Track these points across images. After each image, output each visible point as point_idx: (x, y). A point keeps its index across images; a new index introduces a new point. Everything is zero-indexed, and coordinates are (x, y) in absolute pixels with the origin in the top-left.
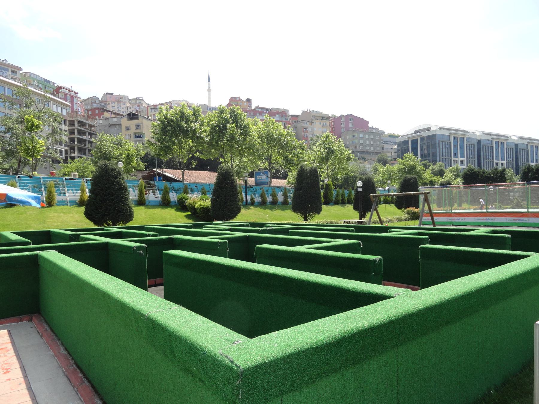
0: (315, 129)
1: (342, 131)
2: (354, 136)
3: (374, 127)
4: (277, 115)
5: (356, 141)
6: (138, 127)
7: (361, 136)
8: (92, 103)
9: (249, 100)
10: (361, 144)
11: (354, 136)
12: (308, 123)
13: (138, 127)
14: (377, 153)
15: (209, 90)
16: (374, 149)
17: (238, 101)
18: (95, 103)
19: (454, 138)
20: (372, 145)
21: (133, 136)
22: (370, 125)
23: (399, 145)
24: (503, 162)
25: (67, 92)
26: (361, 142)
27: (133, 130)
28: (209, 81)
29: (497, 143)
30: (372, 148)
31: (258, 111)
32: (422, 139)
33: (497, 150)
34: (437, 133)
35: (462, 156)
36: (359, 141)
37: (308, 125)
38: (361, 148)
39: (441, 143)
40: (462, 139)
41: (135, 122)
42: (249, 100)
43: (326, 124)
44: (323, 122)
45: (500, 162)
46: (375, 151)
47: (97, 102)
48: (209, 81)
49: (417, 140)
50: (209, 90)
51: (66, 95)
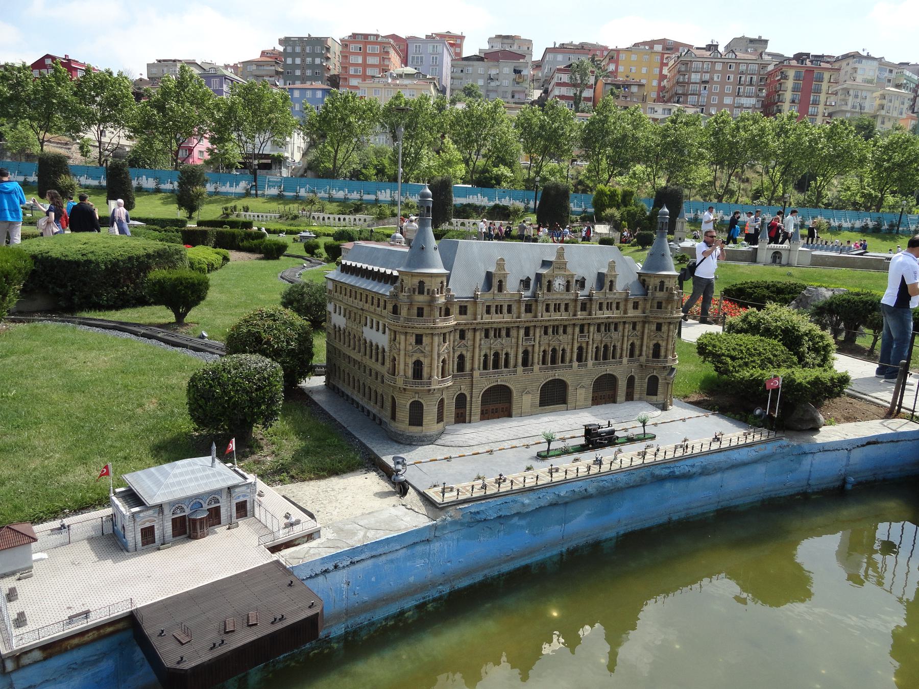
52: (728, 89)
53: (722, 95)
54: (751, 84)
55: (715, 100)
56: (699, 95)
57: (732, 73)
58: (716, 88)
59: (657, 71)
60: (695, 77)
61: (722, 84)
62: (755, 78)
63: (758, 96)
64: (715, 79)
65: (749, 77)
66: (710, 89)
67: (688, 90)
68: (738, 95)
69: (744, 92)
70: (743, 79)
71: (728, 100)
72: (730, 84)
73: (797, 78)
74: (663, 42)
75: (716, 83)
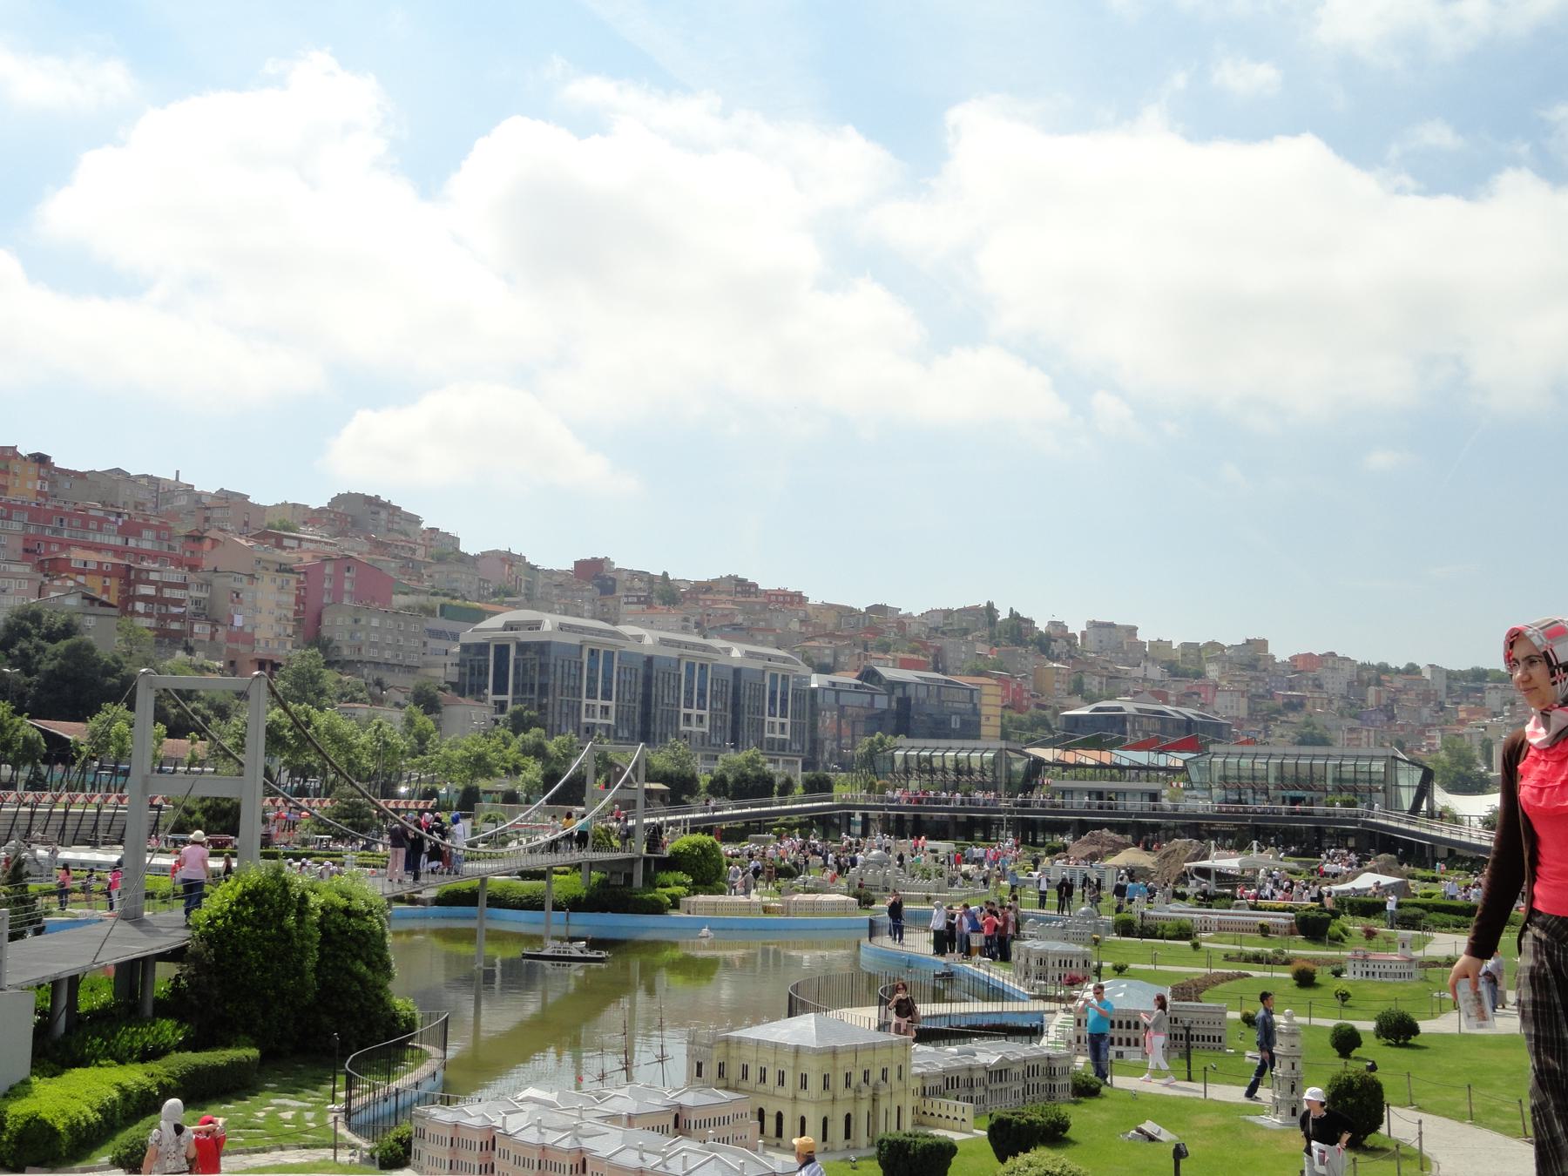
1: (326, 600)
3: (384, 499)
5: (361, 635)
7: (375, 622)
10: (374, 645)
12: (245, 579)
14: (411, 669)
17: (9, 459)
19: (592, 652)
23: (466, 648)
24: (701, 712)
26: (374, 637)
29: (690, 667)
32: (523, 647)
33: (689, 681)
34: (555, 639)
35: (607, 695)
37: (244, 584)
39: (560, 663)
40: (609, 656)
44: (280, 578)
45: (695, 712)
46: (407, 662)
49: (507, 647)
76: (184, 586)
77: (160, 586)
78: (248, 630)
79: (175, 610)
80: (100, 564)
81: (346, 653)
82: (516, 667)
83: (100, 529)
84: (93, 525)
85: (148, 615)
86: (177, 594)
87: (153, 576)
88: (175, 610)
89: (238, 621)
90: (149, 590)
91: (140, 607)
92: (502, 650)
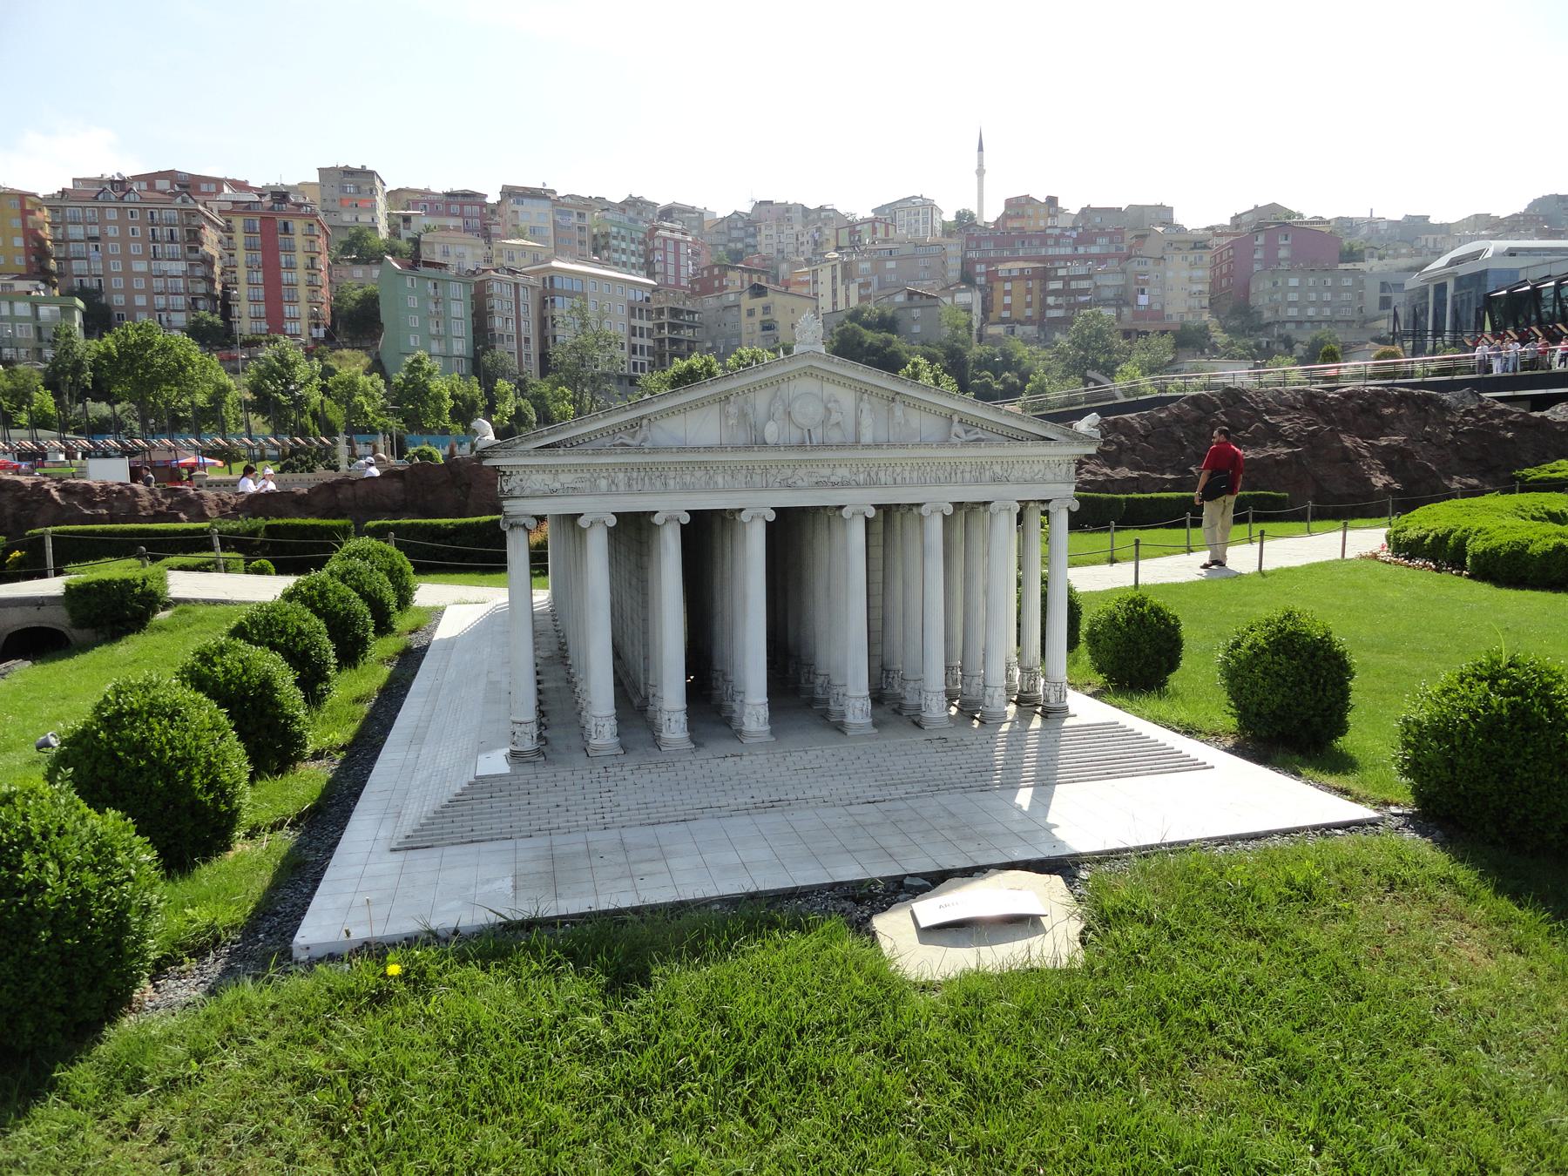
0: (1170, 274)
1: (1257, 267)
2: (1275, 284)
4: (1100, 241)
5: (1278, 297)
6: (766, 309)
7: (1294, 282)
8: (730, 228)
9: (1052, 201)
10: (1292, 304)
11: (1275, 284)
12: (1150, 262)
13: (766, 309)
15: (980, 172)
16: (1333, 313)
18: (736, 228)
20: (1327, 303)
21: (758, 327)
22: (1431, 220)
25: (667, 234)
26: (1293, 297)
27: (759, 316)
28: (981, 149)
30: (1327, 312)
31: (1050, 236)
32: (1459, 281)
34: (1492, 266)
36: (1285, 296)
38: (1293, 312)
41: (762, 301)
42: (1052, 201)
43: (1201, 258)
46: (1338, 317)
47: (740, 225)
48: (981, 149)
50: (980, 172)
51: (665, 239)
52: (136, 249)
53: (127, 258)
54: (172, 239)
55: (116, 266)
56: (87, 259)
57: (136, 223)
58: (114, 248)
59: (17, 223)
60: (76, 232)
61: (124, 240)
62: (177, 230)
63: (186, 259)
64: (111, 234)
65: (166, 231)
66: (105, 248)
67: (67, 251)
68: (155, 258)
69: (163, 253)
70: (158, 233)
71: (140, 266)
72: (136, 240)
73: (249, 230)
74: (170, 175)
75: (113, 239)
76: (1088, 277)
77: (1067, 280)
78: (1156, 307)
79: (1082, 299)
80: (1022, 270)
81: (1267, 316)
82: (1454, 304)
83: (1057, 244)
84: (1051, 242)
85: (1058, 307)
86: (1084, 284)
87: (1061, 272)
88: (1082, 299)
89: (1143, 300)
90: (1057, 285)
91: (1051, 300)
92: (1440, 289)
